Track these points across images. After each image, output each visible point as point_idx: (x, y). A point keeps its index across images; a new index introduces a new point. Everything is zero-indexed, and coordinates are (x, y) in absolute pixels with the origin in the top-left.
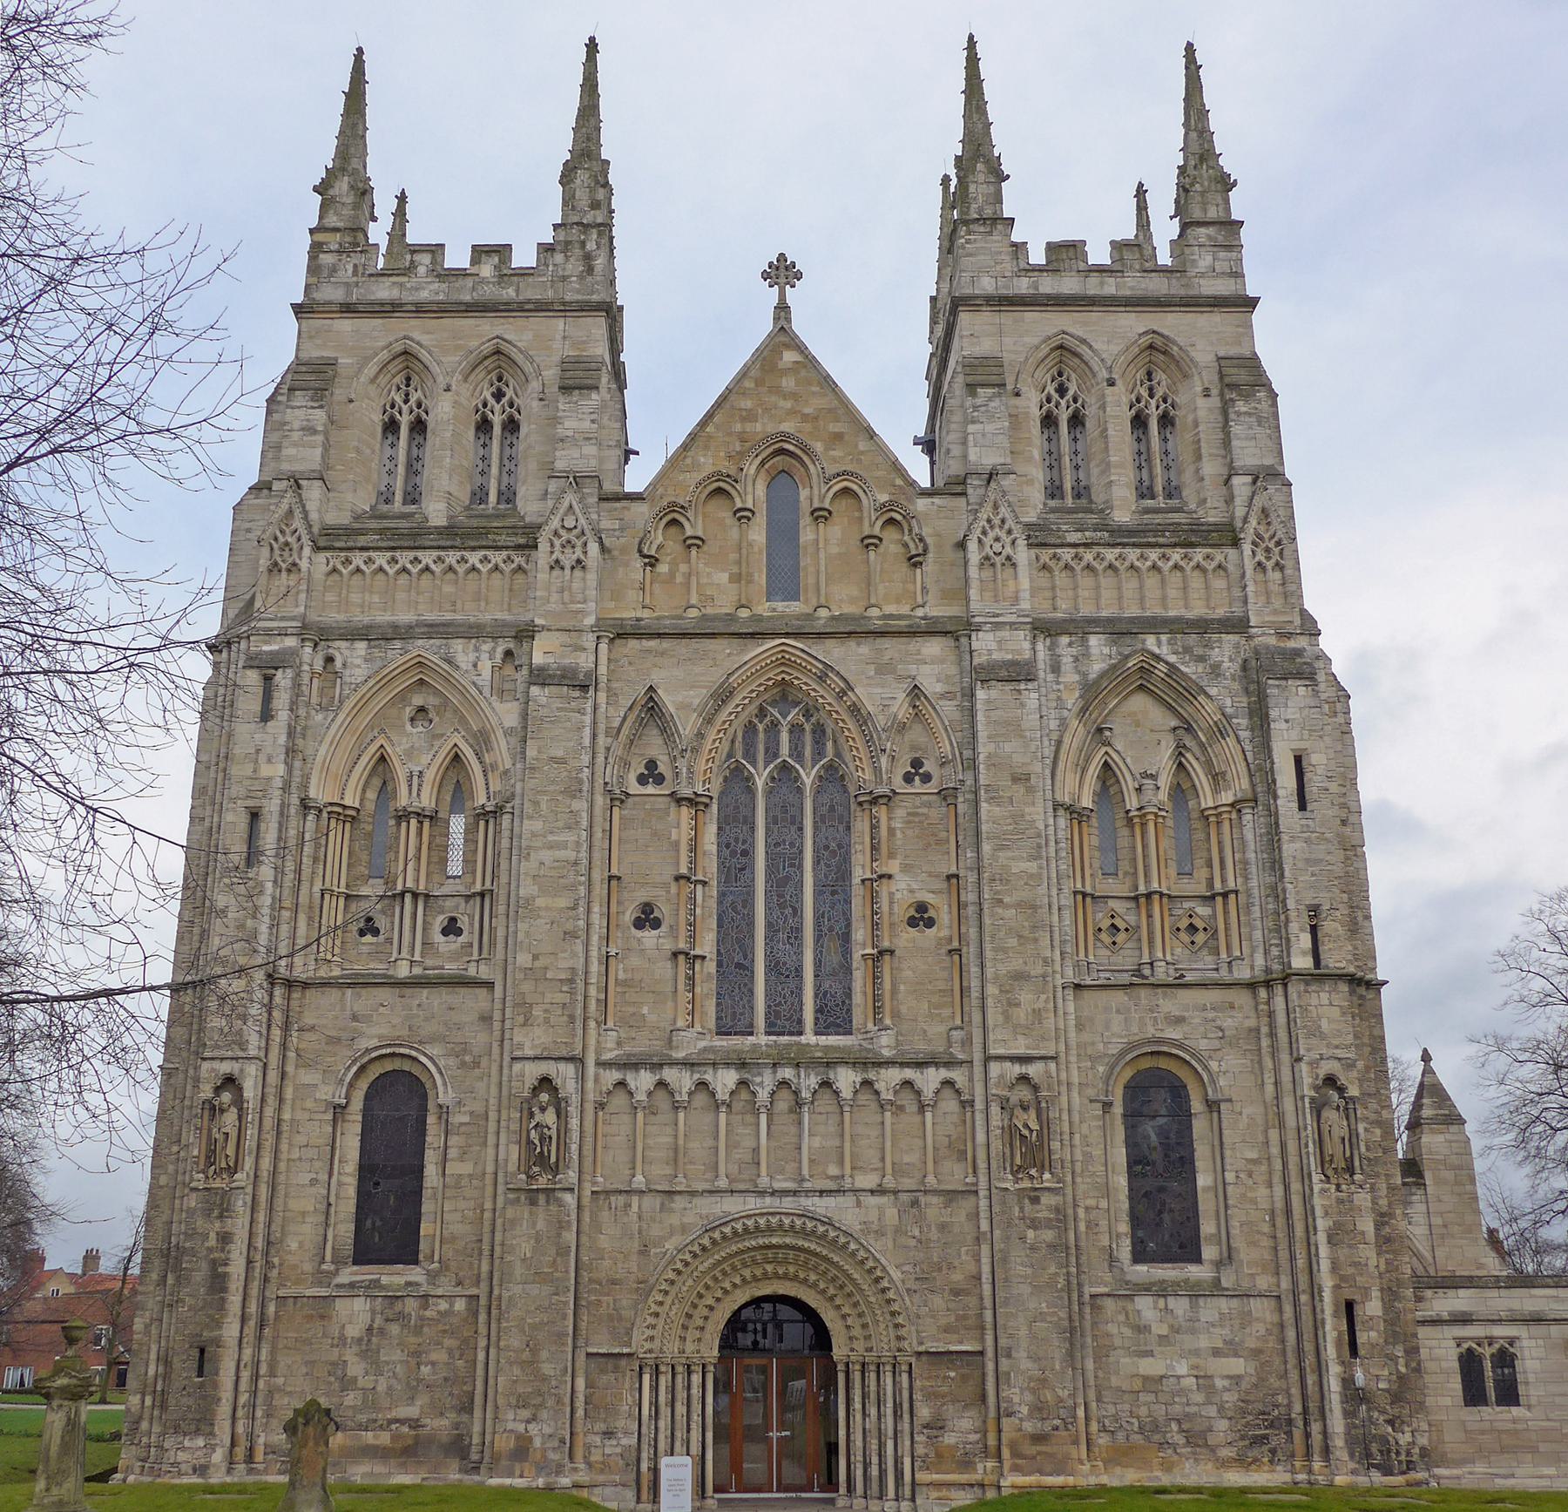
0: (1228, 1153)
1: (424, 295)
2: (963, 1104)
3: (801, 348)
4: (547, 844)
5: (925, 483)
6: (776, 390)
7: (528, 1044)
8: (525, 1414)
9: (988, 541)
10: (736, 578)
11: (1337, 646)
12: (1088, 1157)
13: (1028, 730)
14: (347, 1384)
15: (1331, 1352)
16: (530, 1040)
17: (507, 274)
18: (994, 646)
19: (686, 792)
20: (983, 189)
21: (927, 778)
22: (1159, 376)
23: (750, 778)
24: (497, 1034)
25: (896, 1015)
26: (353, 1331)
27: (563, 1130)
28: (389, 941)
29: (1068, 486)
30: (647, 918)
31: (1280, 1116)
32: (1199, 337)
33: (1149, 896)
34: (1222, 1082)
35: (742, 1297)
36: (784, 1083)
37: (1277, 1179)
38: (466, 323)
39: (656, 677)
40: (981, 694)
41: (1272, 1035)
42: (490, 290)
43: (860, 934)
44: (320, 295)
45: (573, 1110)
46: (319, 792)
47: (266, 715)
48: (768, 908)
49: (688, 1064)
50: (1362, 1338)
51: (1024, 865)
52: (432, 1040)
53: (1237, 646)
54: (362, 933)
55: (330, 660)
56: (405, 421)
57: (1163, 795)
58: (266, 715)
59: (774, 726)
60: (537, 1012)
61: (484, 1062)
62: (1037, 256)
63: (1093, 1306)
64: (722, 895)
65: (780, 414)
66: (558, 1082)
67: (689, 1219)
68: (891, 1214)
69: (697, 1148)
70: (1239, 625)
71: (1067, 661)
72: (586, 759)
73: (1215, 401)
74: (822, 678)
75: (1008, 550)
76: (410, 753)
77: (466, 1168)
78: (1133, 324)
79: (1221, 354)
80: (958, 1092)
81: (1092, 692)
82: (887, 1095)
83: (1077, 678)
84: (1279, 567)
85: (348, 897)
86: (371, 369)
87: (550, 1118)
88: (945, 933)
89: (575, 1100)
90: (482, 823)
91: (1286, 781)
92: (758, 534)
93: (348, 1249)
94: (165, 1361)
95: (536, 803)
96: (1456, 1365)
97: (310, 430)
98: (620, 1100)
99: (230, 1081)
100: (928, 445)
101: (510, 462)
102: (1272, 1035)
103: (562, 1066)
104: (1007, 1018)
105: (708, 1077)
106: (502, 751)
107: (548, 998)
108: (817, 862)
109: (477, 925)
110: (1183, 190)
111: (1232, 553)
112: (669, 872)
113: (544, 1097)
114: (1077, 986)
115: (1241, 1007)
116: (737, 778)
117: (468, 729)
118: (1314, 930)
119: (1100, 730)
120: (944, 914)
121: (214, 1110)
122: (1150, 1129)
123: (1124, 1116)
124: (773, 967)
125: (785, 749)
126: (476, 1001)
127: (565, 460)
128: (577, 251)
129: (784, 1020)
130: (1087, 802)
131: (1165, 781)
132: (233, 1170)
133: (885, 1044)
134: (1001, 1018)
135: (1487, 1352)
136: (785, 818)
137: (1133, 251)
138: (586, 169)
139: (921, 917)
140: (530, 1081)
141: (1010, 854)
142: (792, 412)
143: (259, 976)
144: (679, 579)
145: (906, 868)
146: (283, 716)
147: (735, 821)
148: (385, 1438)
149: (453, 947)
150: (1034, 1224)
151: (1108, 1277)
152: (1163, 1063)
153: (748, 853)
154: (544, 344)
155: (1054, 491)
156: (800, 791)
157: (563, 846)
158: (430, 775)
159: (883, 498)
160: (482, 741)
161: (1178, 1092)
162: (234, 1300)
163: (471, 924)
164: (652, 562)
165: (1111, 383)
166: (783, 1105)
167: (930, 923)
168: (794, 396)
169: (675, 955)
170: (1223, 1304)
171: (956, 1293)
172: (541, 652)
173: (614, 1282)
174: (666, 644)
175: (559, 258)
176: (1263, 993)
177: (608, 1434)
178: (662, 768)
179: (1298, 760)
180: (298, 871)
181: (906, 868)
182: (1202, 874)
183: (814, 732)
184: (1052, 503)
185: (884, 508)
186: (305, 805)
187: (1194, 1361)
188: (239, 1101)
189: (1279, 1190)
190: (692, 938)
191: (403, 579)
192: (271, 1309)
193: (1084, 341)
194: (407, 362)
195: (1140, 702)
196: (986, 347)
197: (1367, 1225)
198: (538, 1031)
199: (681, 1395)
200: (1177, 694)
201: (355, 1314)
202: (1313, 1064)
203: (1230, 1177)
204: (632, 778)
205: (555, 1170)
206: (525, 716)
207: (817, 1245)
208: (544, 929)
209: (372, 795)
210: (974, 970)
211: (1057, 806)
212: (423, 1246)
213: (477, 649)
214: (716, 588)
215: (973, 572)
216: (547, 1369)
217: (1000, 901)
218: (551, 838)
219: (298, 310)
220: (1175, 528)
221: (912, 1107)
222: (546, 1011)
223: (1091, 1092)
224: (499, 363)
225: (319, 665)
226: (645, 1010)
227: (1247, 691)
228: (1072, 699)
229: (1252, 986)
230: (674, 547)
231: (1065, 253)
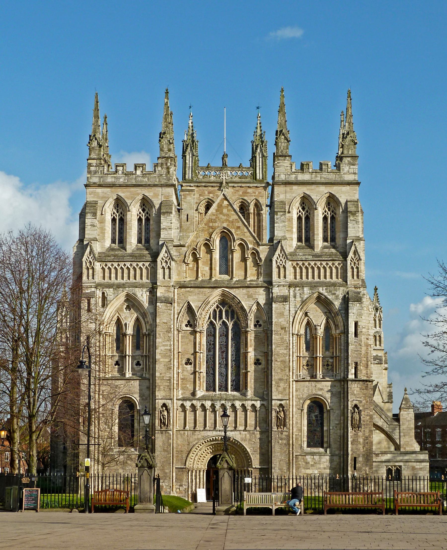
0: (331, 422)
2: (266, 410)
7: (159, 395)
18: (278, 291)
20: (283, 144)
22: (332, 204)
24: (151, 392)
27: (169, 416)
28: (123, 367)
37: (342, 429)
45: (171, 412)
48: (219, 359)
50: (357, 465)
59: (221, 312)
61: (148, 398)
63: (296, 458)
64: (207, 355)
68: (248, 436)
76: (125, 318)
80: (265, 407)
83: (300, 299)
87: (165, 413)
90: (145, 337)
102: (344, 393)
103: (168, 401)
104: (277, 390)
107: (164, 384)
109: (145, 364)
115: (337, 386)
117: (141, 312)
118: (356, 368)
122: (313, 415)
123: (307, 412)
124: (220, 374)
128: (165, 166)
134: (275, 390)
135: (394, 469)
141: (279, 348)
142: (227, 220)
149: (139, 369)
151: (300, 451)
157: (167, 345)
163: (143, 363)
168: (227, 215)
173: (181, 451)
175: (160, 168)
182: (331, 350)
183: (231, 312)
184: (299, 244)
187: (320, 470)
189: (342, 431)
197: (361, 440)
199: (198, 477)
203: (331, 428)
204: (184, 325)
213: (142, 291)
216: (167, 471)
217: (277, 360)
218: (163, 343)
222: (164, 387)
223: (298, 407)
226: (188, 386)
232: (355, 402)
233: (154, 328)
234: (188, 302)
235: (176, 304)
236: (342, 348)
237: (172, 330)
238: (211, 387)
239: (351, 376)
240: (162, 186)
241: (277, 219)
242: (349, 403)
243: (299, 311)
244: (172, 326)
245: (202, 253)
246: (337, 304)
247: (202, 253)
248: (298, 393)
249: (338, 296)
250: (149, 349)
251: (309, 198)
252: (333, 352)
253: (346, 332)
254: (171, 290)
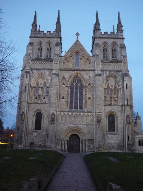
1: (42, 36)
3: (79, 42)
4: (54, 90)
5: (91, 55)
8: (51, 144)
9: (97, 62)
10: (72, 65)
11: (131, 73)
12: (105, 122)
13: (100, 80)
14: (34, 140)
15: (126, 140)
16: (52, 109)
17: (50, 34)
19: (67, 86)
21: (90, 85)
22: (115, 46)
23: (73, 85)
25: (87, 108)
26: (35, 136)
29: (105, 56)
30: (63, 98)
31: (123, 118)
32: (119, 42)
33: (112, 97)
34: (118, 115)
35: (71, 134)
36: (76, 114)
37: (122, 124)
39: (65, 74)
40: (96, 77)
41: (123, 111)
42: (49, 36)
43: (83, 100)
44: (32, 36)
45: (56, 116)
46: (31, 85)
47: (27, 77)
50: (129, 139)
52: (42, 109)
54: (36, 98)
55: (33, 72)
56: (40, 49)
57: (113, 87)
58: (27, 77)
59: (76, 80)
60: (52, 107)
62: (103, 33)
64: (70, 96)
65: (77, 49)
68: (86, 126)
69: (68, 120)
70: (121, 71)
71: (104, 74)
72: (57, 82)
73: (120, 48)
74: (80, 75)
75: (99, 63)
76: (40, 81)
77: (45, 121)
78: (112, 40)
79: (121, 43)
80: (93, 115)
81: (107, 77)
82: (86, 115)
84: (126, 65)
85: (34, 95)
86: (37, 44)
87: (54, 117)
91: (125, 86)
92: (75, 61)
93: (34, 128)
94: (18, 138)
96: (138, 142)
97: (31, 49)
98: (60, 115)
99: (23, 112)
100: (92, 52)
101: (50, 53)
102: (123, 111)
105: (69, 113)
106: (49, 81)
110: (118, 27)
111: (121, 64)
112: (65, 94)
113: (53, 115)
114: (104, 106)
116: (72, 85)
119: (107, 81)
120: (92, 98)
121: (22, 115)
124: (75, 103)
125: (77, 82)
126: (47, 105)
127: (56, 53)
128: (57, 32)
129: (76, 108)
130: (106, 88)
131: (114, 86)
132: (24, 121)
133: (86, 110)
136: (77, 88)
137: (113, 33)
138: (58, 24)
139: (89, 98)
140: (52, 113)
143: (26, 103)
144: (67, 65)
145: (88, 94)
146: (28, 77)
147: (72, 88)
148: (38, 146)
150: (99, 128)
151: (106, 133)
152: (112, 113)
153: (73, 92)
154: (54, 41)
155: (104, 57)
156: (78, 86)
158: (42, 84)
159: (87, 57)
160: (47, 80)
161: (113, 116)
162: (24, 132)
164: (64, 63)
165: (110, 46)
166: (76, 116)
167: (90, 99)
168: (79, 47)
169: (66, 101)
170: (117, 136)
171: (92, 134)
172: (53, 72)
175: (55, 32)
176: (122, 107)
177: (59, 146)
178: (65, 83)
179: (127, 84)
180: (30, 92)
181: (88, 94)
185: (87, 58)
186: (30, 86)
188: (24, 114)
189: (123, 125)
190: (67, 100)
191: (40, 64)
192: (27, 133)
193: (107, 42)
194: (40, 43)
195: (112, 78)
196: (97, 42)
197: (131, 129)
199: (65, 142)
200: (115, 77)
201: (35, 134)
202: (126, 114)
204: (62, 84)
205: (54, 121)
206: (52, 78)
207: (79, 130)
208: (53, 99)
209: (37, 85)
210: (94, 104)
211: (103, 88)
212: (41, 128)
214: (70, 66)
215: (96, 65)
216: (53, 140)
219: (30, 37)
220: (116, 61)
221: (88, 116)
224: (49, 43)
225: (32, 72)
226: (63, 107)
227: (122, 77)
228: (105, 78)
229: (121, 106)
230: (66, 61)
231: (106, 33)
232: (128, 114)
235: (59, 76)
236: (122, 93)
238: (71, 108)
249: (119, 75)
251: (107, 43)
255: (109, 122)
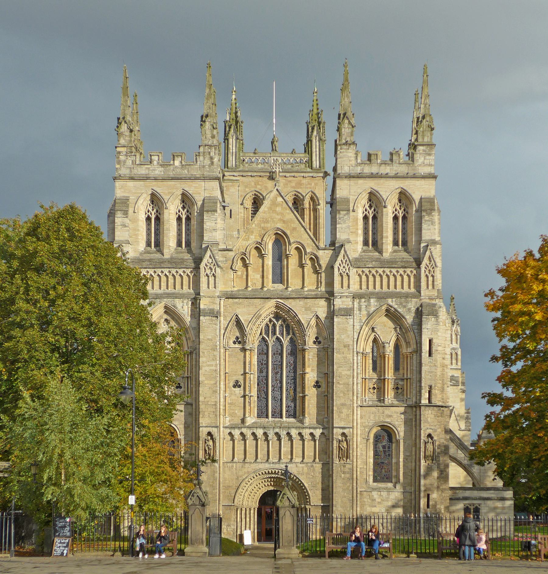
6: (275, 211)
7: (204, 423)
18: (341, 303)
20: (347, 130)
22: (403, 201)
24: (194, 419)
27: (214, 446)
31: (416, 443)
37: (413, 461)
38: (172, 183)
41: (416, 421)
45: (217, 441)
48: (272, 381)
49: (249, 427)
50: (431, 503)
51: (346, 372)
53: (416, 302)
59: (274, 326)
60: (206, 414)
61: (191, 427)
63: (360, 494)
64: (258, 377)
66: (213, 433)
67: (250, 470)
68: (306, 469)
83: (366, 312)
87: (211, 443)
88: (323, 390)
89: (218, 438)
95: (203, 353)
102: (416, 421)
103: (214, 429)
104: (339, 417)
107: (209, 409)
108: (287, 367)
120: (323, 385)
124: (274, 398)
128: (208, 156)
142: (280, 220)
151: (365, 486)
163: (185, 385)
168: (282, 214)
173: (229, 487)
174: (241, 300)
176: (414, 409)
182: (401, 371)
184: (365, 248)
189: (413, 464)
193: (377, 192)
198: (206, 419)
199: (248, 516)
213: (183, 302)
217: (339, 383)
218: (208, 363)
222: (209, 414)
223: (363, 436)
226: (236, 412)
233: (197, 346)
234: (236, 315)
235: (222, 318)
236: (414, 368)
237: (218, 347)
238: (262, 413)
239: (425, 401)
240: (204, 178)
241: (340, 218)
242: (422, 431)
243: (364, 327)
244: (218, 343)
245: (253, 259)
246: (409, 318)
247: (253, 259)
248: (363, 421)
249: (409, 309)
250: (192, 369)
252: (404, 374)
253: (418, 351)
254: (217, 302)
255: (376, 454)
